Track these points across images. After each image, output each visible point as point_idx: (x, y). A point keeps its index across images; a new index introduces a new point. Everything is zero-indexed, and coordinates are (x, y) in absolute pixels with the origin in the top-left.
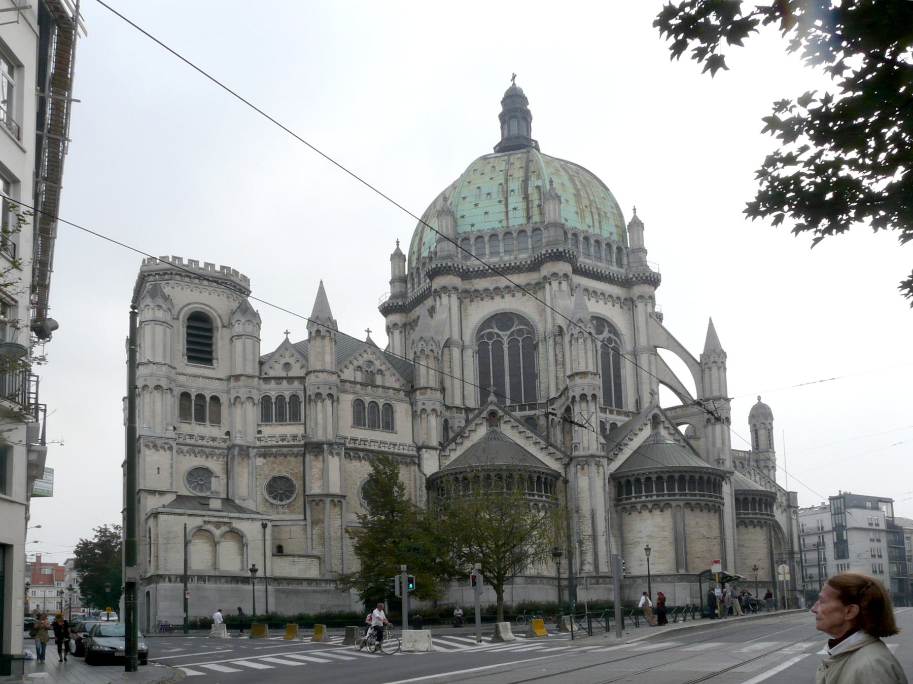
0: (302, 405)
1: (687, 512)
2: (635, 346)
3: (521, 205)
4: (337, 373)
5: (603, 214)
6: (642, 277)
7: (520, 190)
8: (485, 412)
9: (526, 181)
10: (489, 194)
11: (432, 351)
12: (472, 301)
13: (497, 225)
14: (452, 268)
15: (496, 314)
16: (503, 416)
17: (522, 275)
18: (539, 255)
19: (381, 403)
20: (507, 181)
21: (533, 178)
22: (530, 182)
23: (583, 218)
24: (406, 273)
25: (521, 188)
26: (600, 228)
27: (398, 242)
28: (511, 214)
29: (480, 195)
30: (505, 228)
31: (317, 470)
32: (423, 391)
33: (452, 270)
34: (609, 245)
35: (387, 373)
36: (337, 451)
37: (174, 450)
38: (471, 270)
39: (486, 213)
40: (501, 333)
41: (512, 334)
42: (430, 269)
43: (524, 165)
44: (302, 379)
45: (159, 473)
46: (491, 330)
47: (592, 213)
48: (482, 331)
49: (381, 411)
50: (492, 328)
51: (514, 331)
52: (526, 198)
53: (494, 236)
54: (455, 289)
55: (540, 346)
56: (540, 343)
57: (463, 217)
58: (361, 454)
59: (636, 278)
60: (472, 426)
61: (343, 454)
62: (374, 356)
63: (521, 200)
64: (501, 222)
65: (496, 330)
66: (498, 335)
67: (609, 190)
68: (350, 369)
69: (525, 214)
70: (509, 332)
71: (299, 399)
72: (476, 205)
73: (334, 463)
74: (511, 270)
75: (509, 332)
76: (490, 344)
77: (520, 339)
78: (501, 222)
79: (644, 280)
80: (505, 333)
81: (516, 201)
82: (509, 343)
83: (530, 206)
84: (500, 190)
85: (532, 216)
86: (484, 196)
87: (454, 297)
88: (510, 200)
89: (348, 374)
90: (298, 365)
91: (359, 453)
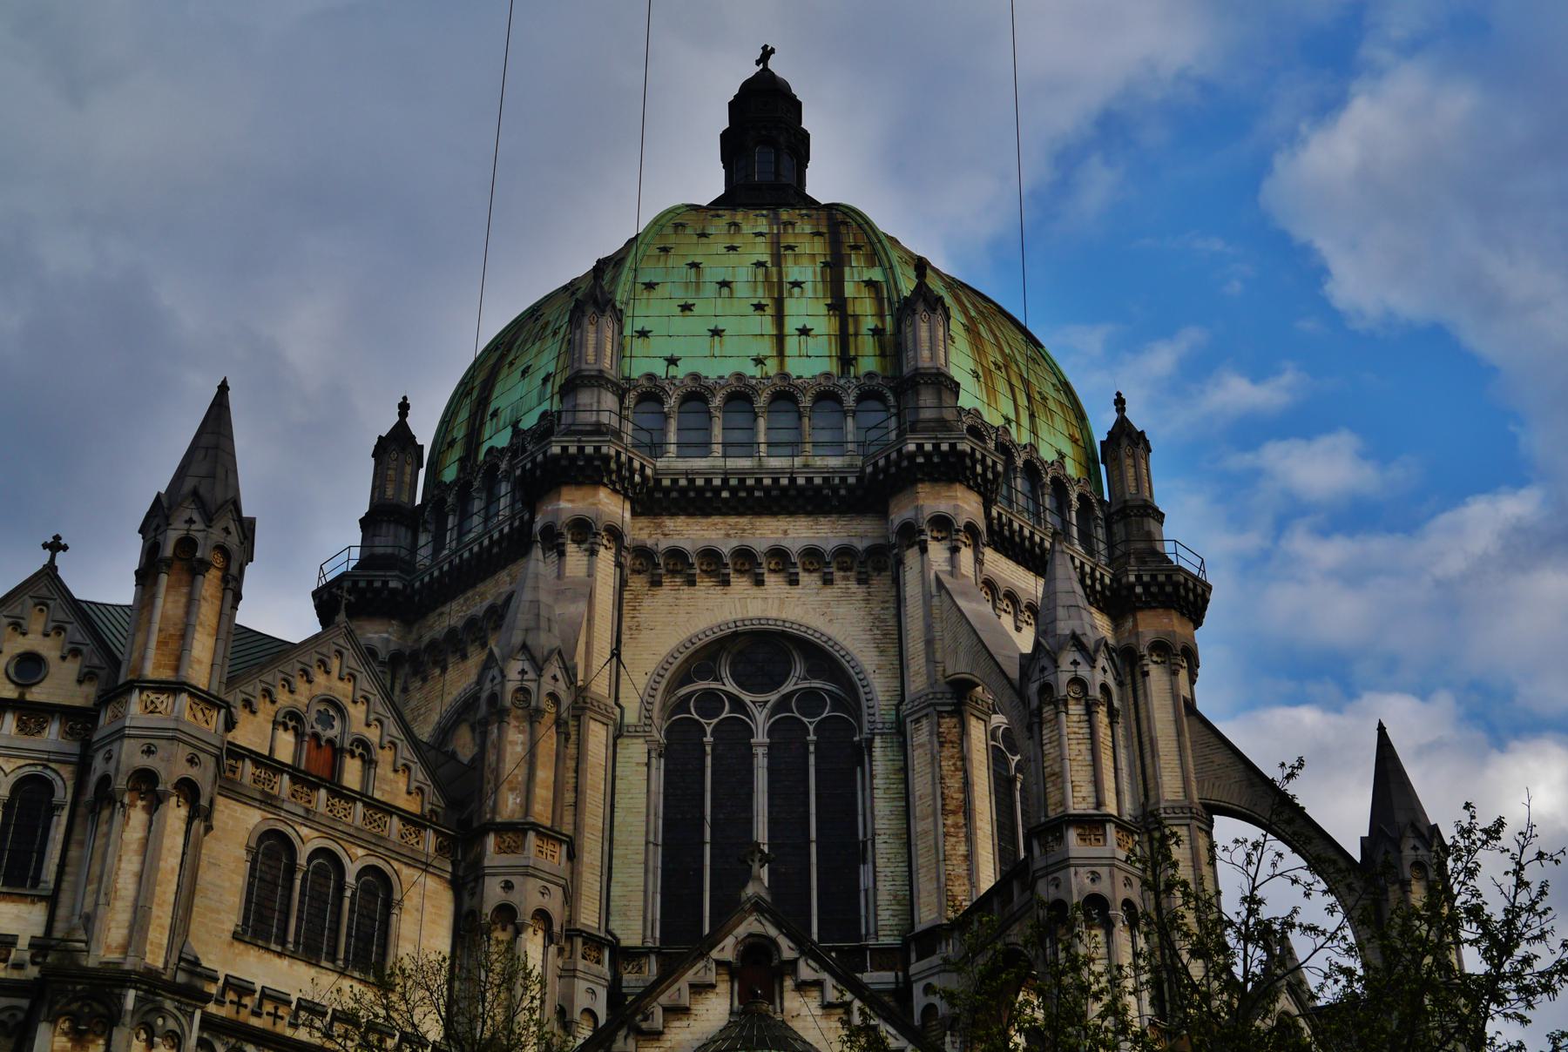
0: (62, 818)
2: (1146, 796)
3: (824, 325)
4: (228, 706)
5: (1037, 397)
7: (820, 286)
8: (729, 941)
10: (724, 284)
11: (553, 696)
12: (656, 583)
13: (751, 370)
14: (613, 466)
15: (735, 634)
16: (794, 962)
18: (894, 456)
19: (355, 860)
20: (778, 259)
21: (856, 260)
22: (847, 270)
24: (418, 501)
25: (824, 281)
26: (1034, 431)
27: (404, 408)
28: (792, 345)
29: (698, 283)
30: (777, 381)
32: (509, 838)
33: (610, 472)
34: (1060, 486)
35: (384, 757)
36: (171, 1024)
38: (666, 482)
39: (716, 333)
40: (747, 698)
41: (783, 703)
42: (540, 458)
44: (79, 720)
46: (714, 685)
48: (682, 684)
49: (348, 893)
50: (718, 679)
52: (838, 306)
53: (740, 396)
54: (615, 534)
56: (878, 742)
57: (643, 334)
59: (1146, 586)
60: (678, 992)
62: (348, 687)
63: (824, 310)
64: (759, 361)
65: (731, 687)
66: (738, 705)
67: (1042, 347)
68: (261, 716)
70: (773, 697)
71: (52, 793)
72: (686, 308)
75: (773, 697)
76: (709, 730)
77: (811, 723)
78: (759, 361)
80: (761, 698)
81: (808, 310)
82: (771, 733)
83: (851, 330)
84: (760, 278)
85: (855, 358)
86: (710, 290)
87: (606, 558)
88: (790, 306)
89: (252, 733)
90: (72, 668)
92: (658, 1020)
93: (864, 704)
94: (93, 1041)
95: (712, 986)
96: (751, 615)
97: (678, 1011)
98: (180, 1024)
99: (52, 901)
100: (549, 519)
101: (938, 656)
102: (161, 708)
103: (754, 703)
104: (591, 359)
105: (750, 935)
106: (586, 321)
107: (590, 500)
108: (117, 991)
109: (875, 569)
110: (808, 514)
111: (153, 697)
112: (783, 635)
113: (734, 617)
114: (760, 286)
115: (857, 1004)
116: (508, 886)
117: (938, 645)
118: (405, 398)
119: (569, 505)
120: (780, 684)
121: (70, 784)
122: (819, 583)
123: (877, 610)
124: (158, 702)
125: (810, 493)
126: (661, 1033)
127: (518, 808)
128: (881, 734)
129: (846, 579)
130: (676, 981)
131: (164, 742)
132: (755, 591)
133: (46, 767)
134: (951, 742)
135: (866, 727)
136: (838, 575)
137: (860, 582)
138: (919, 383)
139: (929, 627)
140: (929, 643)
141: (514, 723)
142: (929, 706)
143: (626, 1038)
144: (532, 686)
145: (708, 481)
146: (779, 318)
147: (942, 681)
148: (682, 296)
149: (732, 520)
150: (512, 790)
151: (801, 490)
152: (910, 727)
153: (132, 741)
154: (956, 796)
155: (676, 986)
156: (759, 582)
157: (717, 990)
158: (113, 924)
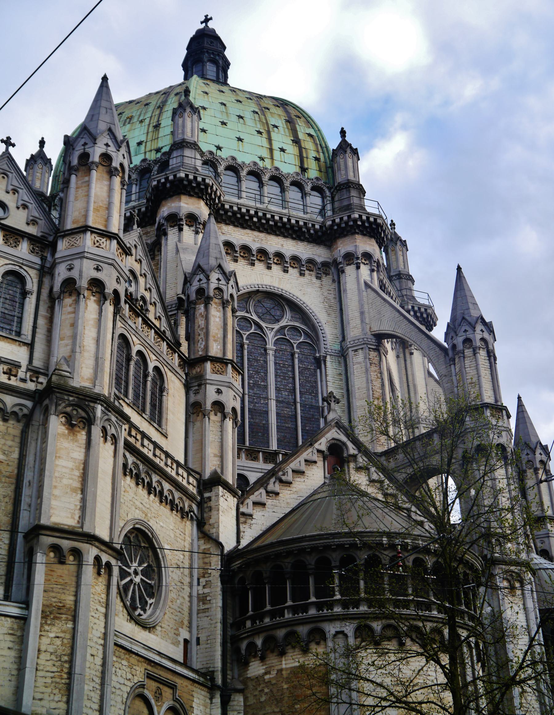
3: (292, 149)
15: (258, 291)
16: (355, 456)
17: (300, 243)
27: (42, 143)
28: (277, 154)
31: (70, 464)
32: (218, 365)
39: (240, 139)
51: (285, 327)
52: (296, 141)
55: (328, 364)
56: (328, 357)
57: (204, 131)
60: (297, 463)
63: (291, 142)
65: (255, 317)
70: (276, 327)
74: (287, 229)
75: (276, 327)
79: (424, 319)
82: (275, 343)
83: (305, 155)
84: (257, 119)
85: (307, 169)
92: (289, 477)
93: (321, 338)
94: (79, 432)
95: (315, 462)
96: (265, 283)
97: (298, 473)
98: (117, 431)
99: (31, 346)
100: (173, 210)
101: (367, 321)
102: (103, 246)
103: (267, 327)
104: (189, 134)
105: (333, 439)
106: (186, 115)
107: (197, 205)
108: (92, 404)
109: (324, 273)
110: (294, 239)
111: (98, 238)
112: (281, 296)
113: (257, 282)
114: (258, 122)
116: (219, 392)
117: (367, 315)
118: (43, 138)
119: (186, 206)
120: (278, 321)
121: (36, 281)
122: (298, 274)
123: (326, 294)
124: (101, 242)
125: (297, 229)
126: (291, 483)
127: (219, 351)
128: (330, 355)
129: (311, 275)
130: (298, 457)
131: (106, 265)
132: (267, 271)
133: (21, 267)
134: (375, 364)
135: (323, 350)
136: (307, 272)
137: (317, 278)
138: (350, 187)
139: (361, 306)
140: (362, 313)
141: (214, 305)
142: (364, 344)
143: (274, 483)
144: (224, 288)
145: (248, 211)
146: (270, 140)
147: (369, 333)
149: (256, 233)
150: (215, 341)
151: (292, 226)
152: (351, 353)
153: (88, 261)
154: (378, 390)
155: (298, 460)
156: (269, 268)
157: (317, 465)
158: (83, 365)
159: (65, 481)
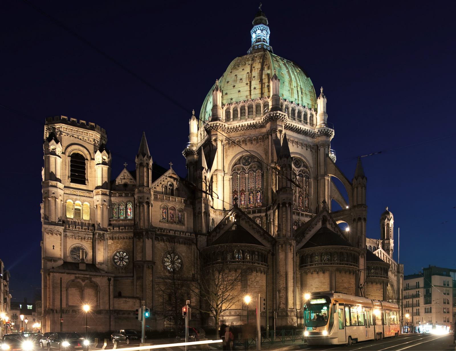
1: (338, 274)
3: (258, 86)
6: (323, 132)
7: (258, 77)
9: (262, 69)
10: (241, 79)
21: (266, 69)
23: (292, 93)
25: (259, 76)
28: (253, 92)
29: (236, 80)
31: (140, 247)
37: (62, 235)
39: (239, 91)
43: (261, 61)
45: (54, 249)
47: (298, 91)
58: (165, 238)
61: (154, 238)
63: (258, 82)
69: (260, 92)
73: (149, 243)
83: (263, 87)
85: (264, 93)
88: (253, 83)
91: (164, 237)
115: (250, 221)
148: (233, 84)
159: (139, 251)
